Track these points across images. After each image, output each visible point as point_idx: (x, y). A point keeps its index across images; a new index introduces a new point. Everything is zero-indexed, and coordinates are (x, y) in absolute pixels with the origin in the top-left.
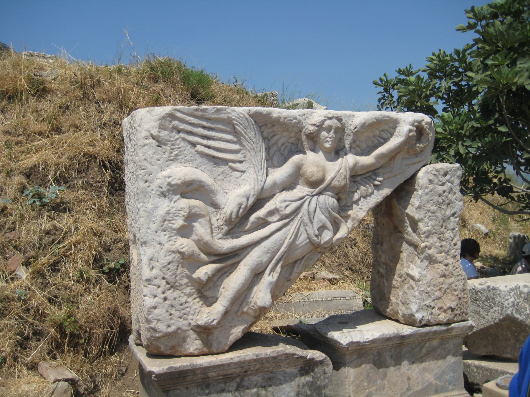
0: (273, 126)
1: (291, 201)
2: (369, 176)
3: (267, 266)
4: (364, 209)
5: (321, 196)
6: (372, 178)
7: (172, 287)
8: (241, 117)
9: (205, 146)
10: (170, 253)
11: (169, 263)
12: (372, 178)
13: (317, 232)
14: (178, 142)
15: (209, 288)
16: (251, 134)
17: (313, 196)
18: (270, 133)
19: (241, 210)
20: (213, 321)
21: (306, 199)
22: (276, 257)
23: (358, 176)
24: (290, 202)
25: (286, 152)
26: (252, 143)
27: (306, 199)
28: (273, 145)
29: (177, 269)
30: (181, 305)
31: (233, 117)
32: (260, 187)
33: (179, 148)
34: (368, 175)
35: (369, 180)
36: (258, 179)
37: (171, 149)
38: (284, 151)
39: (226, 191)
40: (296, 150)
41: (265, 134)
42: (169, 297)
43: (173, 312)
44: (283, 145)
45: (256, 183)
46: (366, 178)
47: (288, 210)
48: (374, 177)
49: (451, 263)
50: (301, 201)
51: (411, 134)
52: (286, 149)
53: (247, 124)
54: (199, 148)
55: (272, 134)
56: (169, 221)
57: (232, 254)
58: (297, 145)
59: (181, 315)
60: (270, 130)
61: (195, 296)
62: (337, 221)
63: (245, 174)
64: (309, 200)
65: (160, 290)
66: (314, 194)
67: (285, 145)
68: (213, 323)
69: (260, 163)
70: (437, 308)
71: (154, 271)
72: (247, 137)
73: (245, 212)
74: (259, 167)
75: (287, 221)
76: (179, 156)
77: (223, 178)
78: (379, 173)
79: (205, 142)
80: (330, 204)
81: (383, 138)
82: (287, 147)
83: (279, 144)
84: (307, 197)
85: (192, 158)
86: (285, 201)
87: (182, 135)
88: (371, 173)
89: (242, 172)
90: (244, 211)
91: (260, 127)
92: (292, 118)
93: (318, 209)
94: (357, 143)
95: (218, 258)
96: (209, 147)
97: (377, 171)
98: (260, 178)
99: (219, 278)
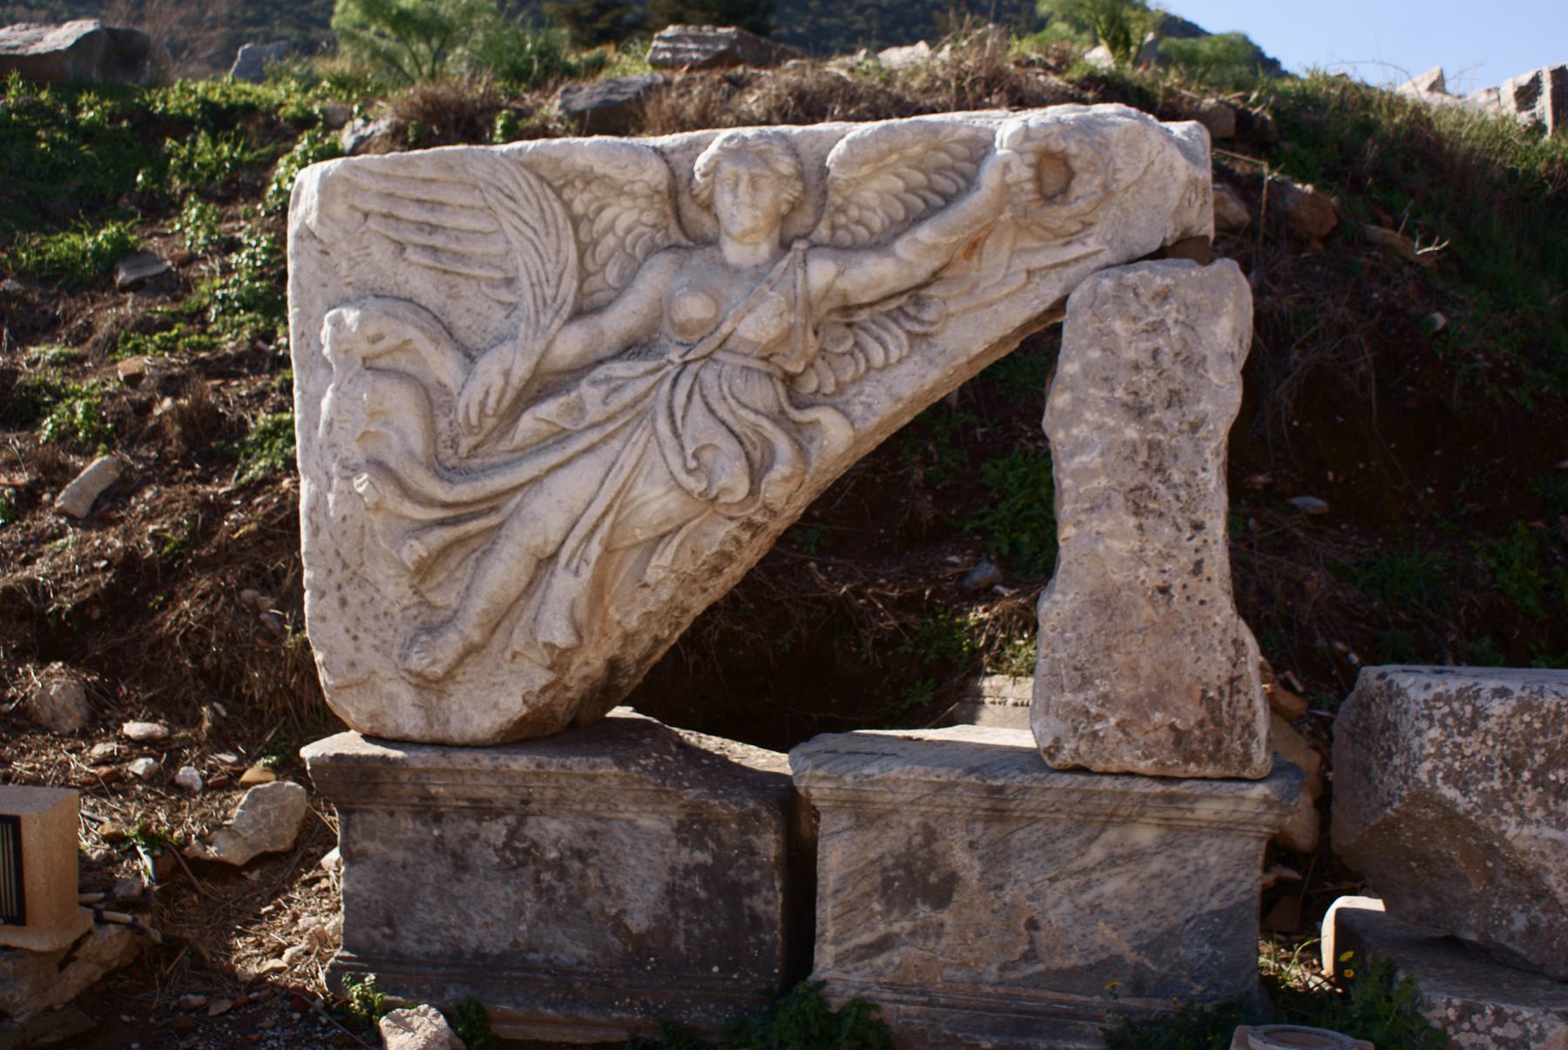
0: (588, 183)
2: (900, 308)
3: (563, 542)
4: (876, 407)
5: (711, 364)
6: (907, 315)
9: (424, 247)
11: (344, 519)
12: (907, 315)
13: (692, 464)
15: (439, 585)
16: (531, 215)
17: (686, 364)
18: (590, 202)
19: (492, 402)
20: (434, 663)
21: (668, 374)
22: (583, 521)
23: (861, 307)
25: (639, 253)
26: (530, 234)
27: (668, 374)
28: (605, 233)
29: (363, 534)
30: (376, 618)
32: (539, 346)
34: (893, 304)
35: (896, 321)
36: (538, 321)
38: (634, 248)
40: (666, 244)
41: (578, 207)
42: (351, 600)
43: (361, 635)
44: (628, 231)
45: (531, 332)
46: (888, 314)
47: (616, 403)
48: (912, 311)
49: (1177, 582)
50: (652, 379)
51: (1010, 178)
54: (410, 254)
57: (484, 506)
58: (667, 228)
59: (376, 642)
60: (587, 196)
61: (406, 602)
64: (673, 375)
65: (332, 581)
66: (688, 358)
67: (636, 232)
68: (434, 669)
69: (553, 283)
70: (1113, 721)
73: (505, 403)
74: (549, 292)
75: (610, 428)
77: (469, 322)
78: (931, 297)
80: (735, 389)
81: (943, 195)
82: (642, 235)
83: (620, 231)
84: (670, 367)
86: (608, 379)
87: (372, 224)
88: (904, 298)
90: (499, 402)
91: (558, 193)
93: (697, 398)
94: (854, 212)
95: (450, 513)
96: (434, 250)
97: (923, 292)
98: (544, 321)
99: (460, 563)
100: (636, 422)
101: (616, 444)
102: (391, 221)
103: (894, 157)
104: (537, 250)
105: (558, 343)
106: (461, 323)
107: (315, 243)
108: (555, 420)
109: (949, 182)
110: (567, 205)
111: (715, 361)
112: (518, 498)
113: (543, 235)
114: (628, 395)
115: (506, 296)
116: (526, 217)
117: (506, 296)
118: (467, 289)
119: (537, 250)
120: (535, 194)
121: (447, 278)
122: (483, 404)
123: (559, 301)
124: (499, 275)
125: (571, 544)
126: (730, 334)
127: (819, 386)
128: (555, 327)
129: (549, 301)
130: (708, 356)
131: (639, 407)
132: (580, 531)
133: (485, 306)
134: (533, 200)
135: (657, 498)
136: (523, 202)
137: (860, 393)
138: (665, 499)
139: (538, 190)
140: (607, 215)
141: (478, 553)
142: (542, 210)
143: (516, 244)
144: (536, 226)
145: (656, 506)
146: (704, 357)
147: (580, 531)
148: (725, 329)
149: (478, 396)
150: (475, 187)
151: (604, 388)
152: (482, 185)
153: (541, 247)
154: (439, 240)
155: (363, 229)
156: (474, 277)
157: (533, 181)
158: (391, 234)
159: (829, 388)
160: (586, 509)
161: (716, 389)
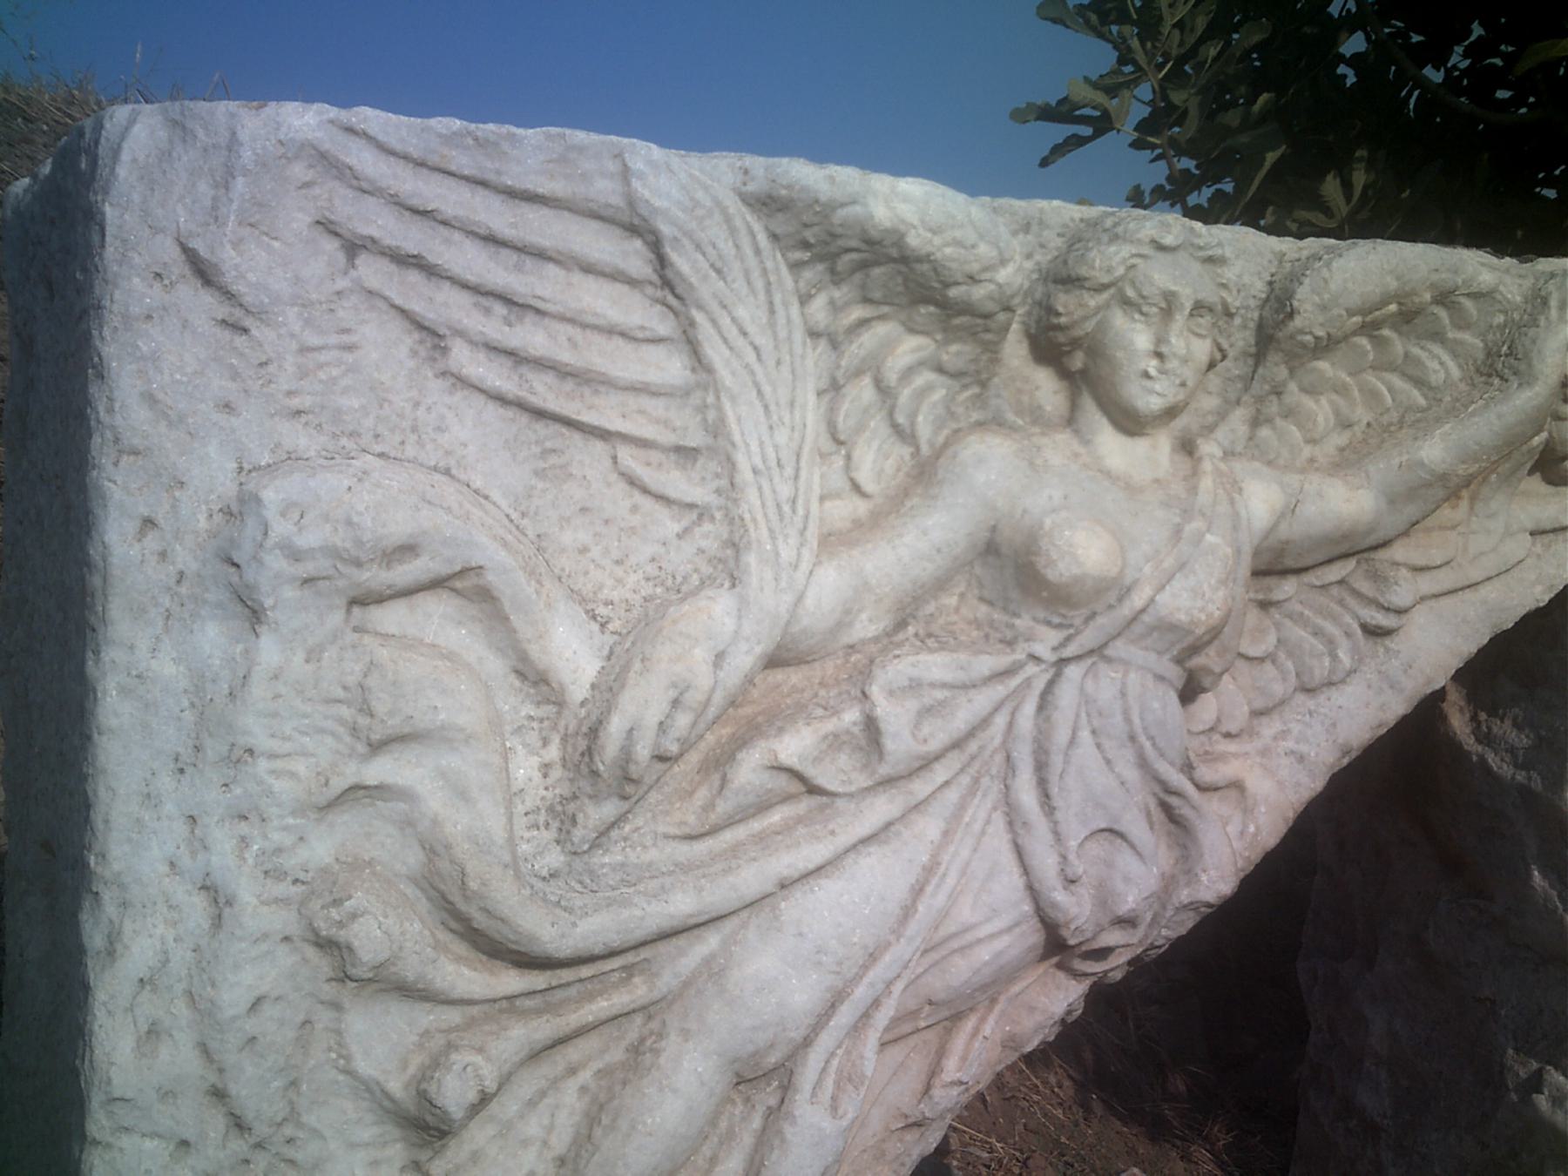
1: (944, 685)
2: (1341, 582)
7: (259, 1146)
8: (697, 204)
9: (494, 349)
10: (264, 947)
14: (344, 314)
17: (1062, 662)
24: (940, 694)
26: (751, 357)
31: (657, 203)
33: (350, 348)
37: (304, 350)
38: (912, 416)
39: (602, 610)
40: (976, 416)
48: (1365, 587)
50: (999, 690)
52: (925, 408)
53: (727, 248)
54: (462, 357)
55: (858, 312)
56: (273, 756)
58: (983, 384)
62: (1186, 811)
63: (707, 527)
64: (1040, 684)
66: (1069, 651)
69: (789, 471)
71: (165, 1052)
72: (725, 321)
75: (921, 787)
76: (345, 391)
77: (584, 537)
78: (1396, 564)
79: (493, 326)
82: (929, 388)
84: (1031, 669)
85: (421, 412)
87: (371, 271)
88: (1351, 564)
89: (691, 506)
92: (970, 236)
96: (515, 357)
98: (787, 553)
99: (532, 1104)
100: (965, 780)
101: (930, 827)
102: (414, 276)
103: (1393, 307)
104: (759, 392)
105: (809, 602)
106: (567, 538)
107: (207, 298)
108: (811, 772)
109: (1434, 365)
110: (805, 299)
111: (1109, 660)
112: (711, 941)
113: (771, 363)
114: (962, 718)
115: (676, 482)
116: (741, 312)
117: (676, 482)
118: (589, 458)
119: (759, 392)
120: (765, 272)
121: (542, 429)
122: (662, 727)
123: (801, 512)
124: (667, 438)
125: (826, 1040)
126: (1143, 611)
127: (1219, 720)
128: (805, 566)
129: (786, 508)
130: (1097, 652)
131: (973, 747)
132: (845, 1016)
133: (627, 503)
134: (759, 284)
135: (992, 936)
136: (740, 284)
137: (1284, 734)
138: (1005, 940)
139: (769, 264)
140: (868, 340)
141: (585, 1076)
142: (772, 311)
143: (724, 373)
144: (761, 340)
145: (984, 954)
146: (1091, 652)
147: (845, 1016)
148: (1138, 600)
149: (653, 717)
150: (633, 230)
151: (912, 705)
152: (665, 229)
153: (767, 389)
154: (532, 337)
155: (342, 283)
156: (604, 435)
157: (762, 238)
158: (416, 306)
159: (1238, 718)
160: (865, 968)
161: (1119, 718)
